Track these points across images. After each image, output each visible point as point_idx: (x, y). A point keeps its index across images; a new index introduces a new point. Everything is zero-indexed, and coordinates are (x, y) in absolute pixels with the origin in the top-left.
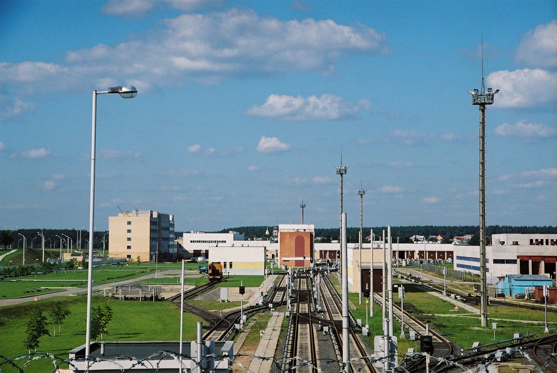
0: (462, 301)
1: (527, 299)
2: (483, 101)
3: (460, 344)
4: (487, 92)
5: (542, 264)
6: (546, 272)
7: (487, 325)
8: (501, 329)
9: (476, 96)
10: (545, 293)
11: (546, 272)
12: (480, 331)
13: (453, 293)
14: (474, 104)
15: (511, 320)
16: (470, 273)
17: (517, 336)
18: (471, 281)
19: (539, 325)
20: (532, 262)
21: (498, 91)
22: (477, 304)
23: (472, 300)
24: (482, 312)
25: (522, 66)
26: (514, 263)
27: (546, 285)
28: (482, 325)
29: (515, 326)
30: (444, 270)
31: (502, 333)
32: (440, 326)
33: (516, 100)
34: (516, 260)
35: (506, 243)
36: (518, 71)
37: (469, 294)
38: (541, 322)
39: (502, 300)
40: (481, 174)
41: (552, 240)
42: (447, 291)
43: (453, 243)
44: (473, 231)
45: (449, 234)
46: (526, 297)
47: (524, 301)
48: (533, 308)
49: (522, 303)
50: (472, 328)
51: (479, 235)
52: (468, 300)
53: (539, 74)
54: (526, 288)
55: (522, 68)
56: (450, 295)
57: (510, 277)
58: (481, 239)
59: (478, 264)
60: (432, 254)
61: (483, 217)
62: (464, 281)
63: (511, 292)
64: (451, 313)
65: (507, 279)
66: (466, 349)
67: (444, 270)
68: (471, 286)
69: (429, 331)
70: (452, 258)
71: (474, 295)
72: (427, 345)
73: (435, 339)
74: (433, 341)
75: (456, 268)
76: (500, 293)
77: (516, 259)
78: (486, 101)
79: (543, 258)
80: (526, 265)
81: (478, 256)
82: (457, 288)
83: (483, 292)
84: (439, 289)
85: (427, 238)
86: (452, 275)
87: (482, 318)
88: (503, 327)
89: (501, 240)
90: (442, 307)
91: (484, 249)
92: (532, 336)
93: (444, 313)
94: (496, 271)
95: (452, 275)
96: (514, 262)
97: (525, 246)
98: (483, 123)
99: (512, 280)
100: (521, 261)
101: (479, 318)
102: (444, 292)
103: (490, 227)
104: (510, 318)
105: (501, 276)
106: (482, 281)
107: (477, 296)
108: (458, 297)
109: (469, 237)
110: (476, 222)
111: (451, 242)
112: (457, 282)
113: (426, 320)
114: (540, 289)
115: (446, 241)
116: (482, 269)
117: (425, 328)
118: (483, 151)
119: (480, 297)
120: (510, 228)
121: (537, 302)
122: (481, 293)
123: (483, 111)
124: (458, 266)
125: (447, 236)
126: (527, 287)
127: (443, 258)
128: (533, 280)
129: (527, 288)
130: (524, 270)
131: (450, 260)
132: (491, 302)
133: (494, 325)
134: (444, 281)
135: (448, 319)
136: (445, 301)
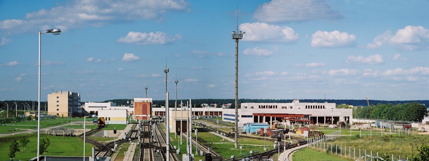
4: (239, 33)
5: (264, 118)
9: (234, 35)
10: (265, 131)
16: (230, 122)
17: (251, 152)
27: (266, 128)
29: (251, 147)
32: (215, 149)
33: (253, 38)
39: (245, 135)
44: (232, 101)
45: (220, 103)
48: (259, 139)
49: (254, 136)
50: (231, 149)
51: (234, 104)
55: (255, 22)
57: (249, 124)
59: (234, 118)
60: (212, 113)
61: (237, 94)
64: (221, 142)
65: (247, 125)
69: (210, 151)
71: (232, 133)
75: (223, 120)
79: (265, 114)
80: (257, 118)
81: (234, 114)
82: (224, 130)
84: (215, 130)
85: (209, 105)
86: (221, 123)
87: (236, 144)
91: (237, 110)
92: (258, 152)
94: (242, 121)
95: (221, 123)
96: (251, 116)
97: (256, 109)
99: (250, 125)
100: (254, 116)
102: (217, 132)
104: (248, 144)
108: (224, 134)
109: (230, 104)
110: (233, 97)
111: (221, 107)
112: (224, 127)
114: (263, 129)
115: (219, 106)
118: (237, 62)
120: (250, 100)
121: (261, 136)
123: (237, 42)
124: (225, 119)
125: (219, 104)
126: (257, 128)
127: (217, 115)
130: (256, 121)
132: (240, 136)
133: (241, 147)
136: (218, 136)
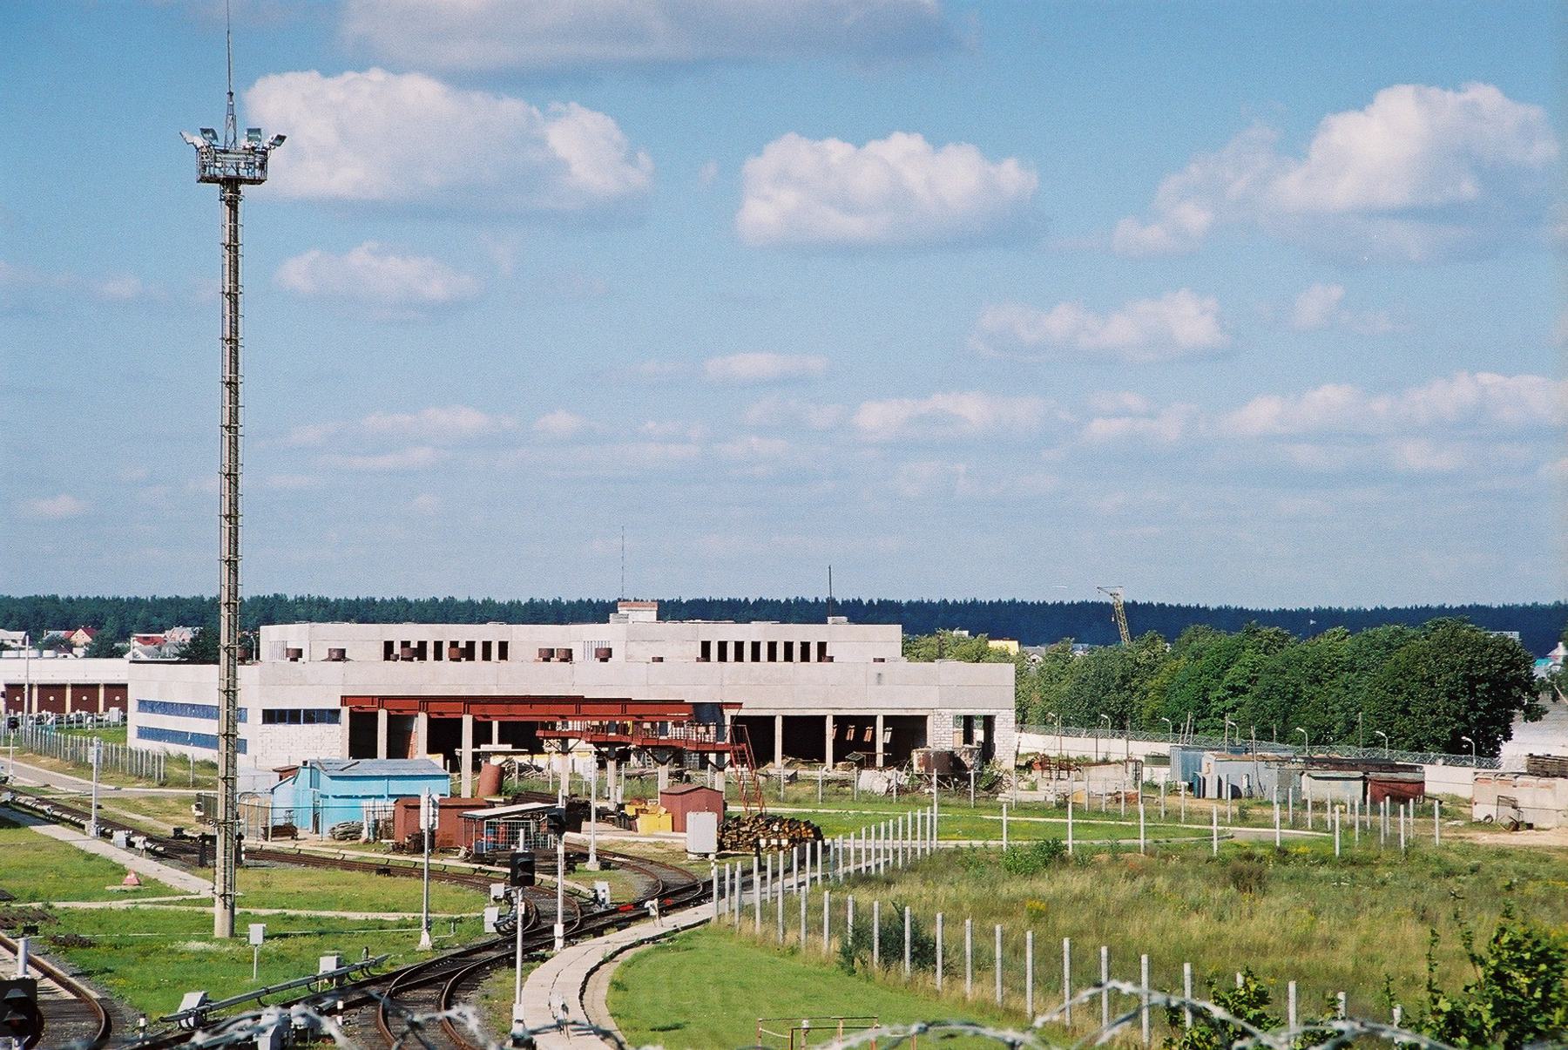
0: (159, 856)
1: (367, 841)
2: (233, 173)
3: (137, 1002)
4: (243, 142)
5: (420, 726)
6: (431, 749)
7: (232, 934)
8: (276, 943)
9: (212, 153)
10: (426, 819)
11: (430, 751)
12: (209, 953)
13: (124, 828)
14: (204, 180)
15: (313, 913)
16: (183, 759)
17: (328, 964)
18: (186, 785)
19: (402, 924)
20: (389, 716)
21: (281, 138)
22: (202, 864)
23: (186, 851)
24: (219, 889)
25: (362, 59)
26: (330, 722)
27: (429, 793)
28: (217, 935)
29: (325, 932)
30: (93, 750)
31: (281, 958)
32: (67, 944)
33: (347, 177)
34: (337, 712)
35: (304, 653)
36: (350, 76)
37: (178, 831)
38: (409, 916)
39: (285, 845)
40: (227, 423)
41: (454, 644)
42: (101, 821)
43: (129, 656)
44: (198, 613)
45: (113, 624)
46: (365, 834)
47: (358, 847)
48: (385, 870)
49: (352, 855)
50: (180, 945)
51: (215, 630)
52: (173, 848)
53: (420, 92)
54: (365, 803)
55: (362, 68)
56: (110, 836)
57: (313, 767)
58: (224, 641)
59: (210, 727)
60: (51, 694)
61: (232, 564)
62: (162, 785)
63: (316, 817)
64: (111, 896)
65: (304, 774)
66: (155, 1017)
67: (93, 750)
68: (186, 801)
69: (30, 961)
70: (124, 709)
71: (194, 830)
72: (17, 1011)
73: (49, 991)
74: (41, 997)
75: (134, 742)
76: (280, 822)
77: (337, 706)
78: (243, 173)
79: (425, 701)
80: (370, 728)
81: (214, 698)
82: (137, 809)
83: (225, 822)
84: (71, 814)
85: (34, 641)
86: (118, 765)
87: (219, 912)
88: (286, 936)
89: (293, 645)
90: (81, 877)
91: (232, 676)
92: (377, 964)
93: (85, 898)
94: (269, 748)
95: (118, 765)
96: (331, 716)
97: (366, 666)
98: (233, 247)
99: (324, 778)
100: (352, 713)
101: (209, 910)
102: (91, 826)
103: (254, 600)
104: (310, 905)
105: (284, 764)
106: (221, 785)
107: (204, 837)
108: (139, 841)
109: (182, 635)
110: (205, 582)
111: (119, 654)
112: (136, 790)
113: (20, 925)
114: (410, 805)
115: (105, 649)
116: (223, 742)
117: (15, 952)
118: (233, 341)
119: (213, 839)
120: (323, 603)
121: (399, 848)
122: (217, 823)
123: (233, 205)
124: (144, 733)
125: (108, 631)
126: (371, 795)
127: (92, 707)
128: (389, 777)
129: (370, 802)
130: (361, 745)
131: (114, 714)
132: (251, 853)
133: (256, 933)
134: (93, 788)
135: (100, 920)
136: (90, 857)
